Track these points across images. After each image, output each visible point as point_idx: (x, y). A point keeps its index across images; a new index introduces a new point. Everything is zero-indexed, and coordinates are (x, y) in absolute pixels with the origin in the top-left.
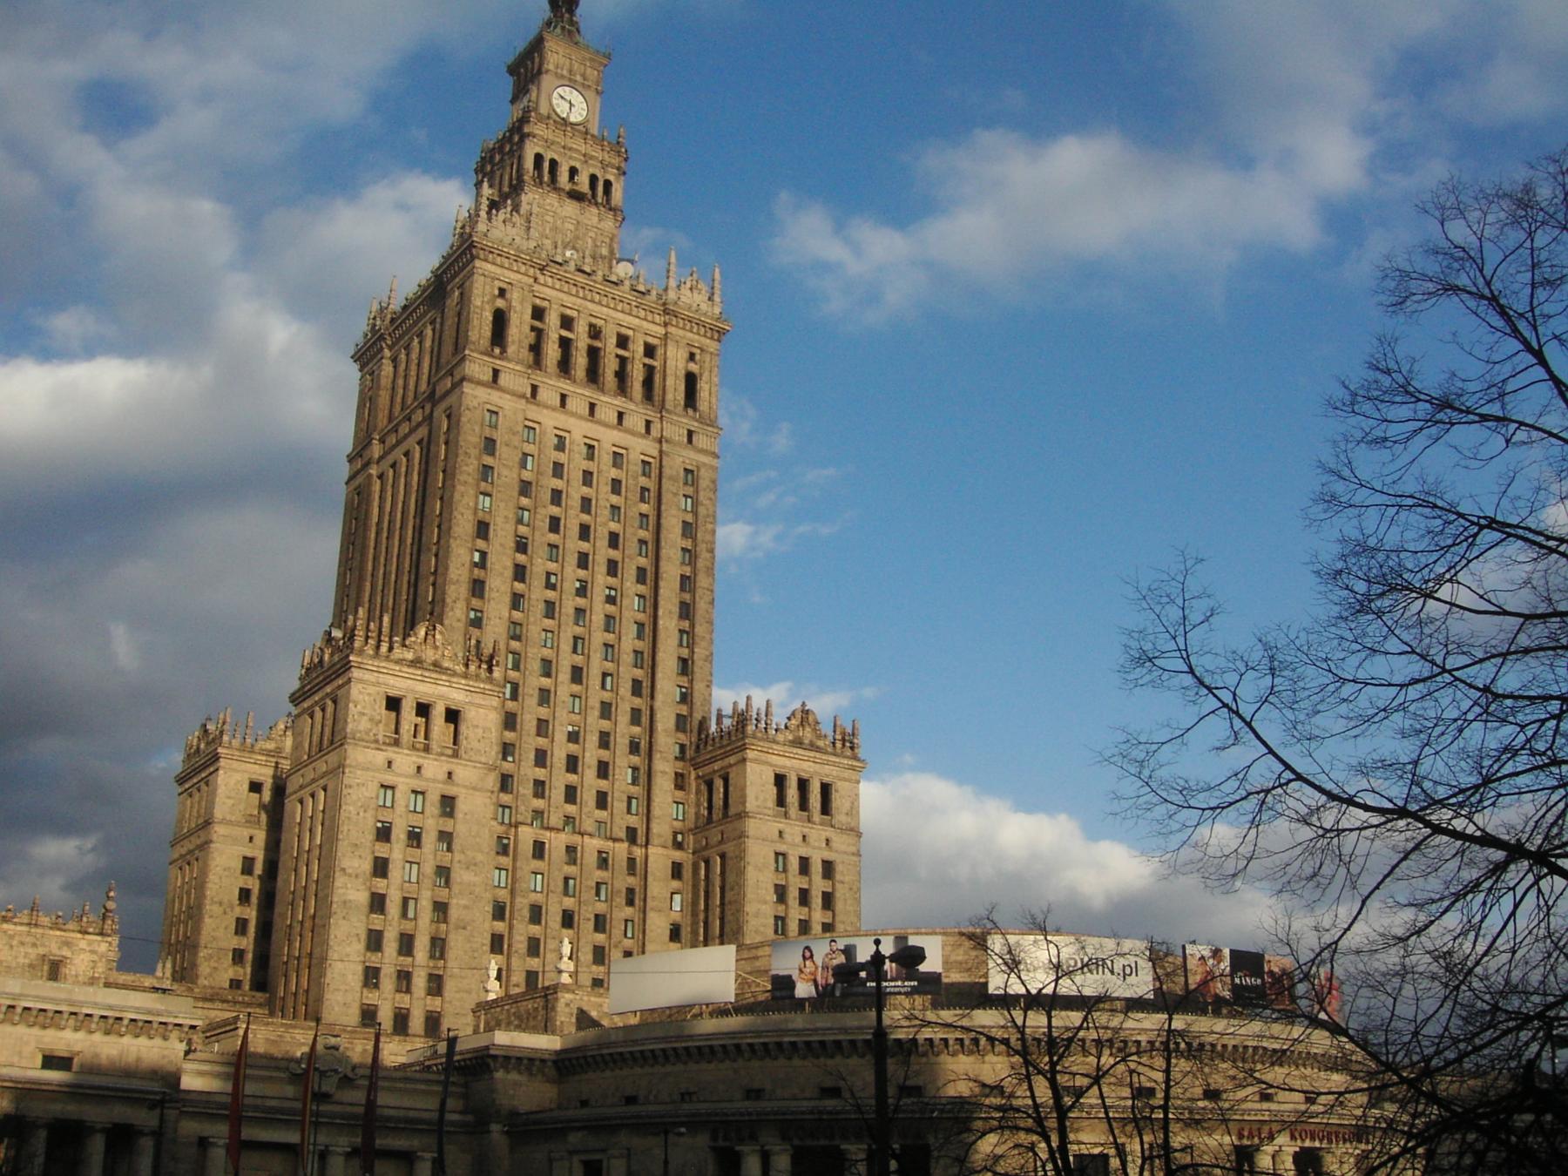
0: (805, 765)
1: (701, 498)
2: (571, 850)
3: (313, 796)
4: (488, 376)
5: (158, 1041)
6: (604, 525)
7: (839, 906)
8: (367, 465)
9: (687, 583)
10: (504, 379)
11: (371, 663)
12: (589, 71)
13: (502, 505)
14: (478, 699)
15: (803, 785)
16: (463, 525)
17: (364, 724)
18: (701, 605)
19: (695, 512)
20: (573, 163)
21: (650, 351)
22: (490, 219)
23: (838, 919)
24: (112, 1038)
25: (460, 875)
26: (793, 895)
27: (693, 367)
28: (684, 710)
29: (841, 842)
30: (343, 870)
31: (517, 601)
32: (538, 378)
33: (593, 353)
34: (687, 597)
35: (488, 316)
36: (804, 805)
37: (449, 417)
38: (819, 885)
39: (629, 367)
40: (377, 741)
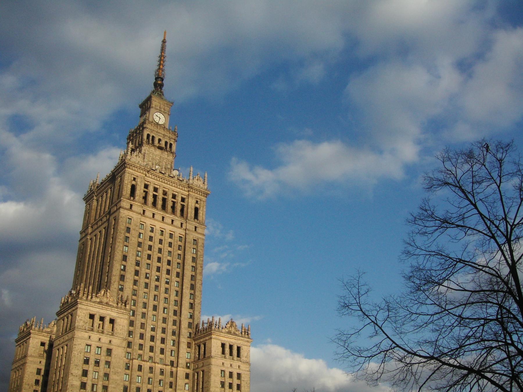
2: (151, 368)
3: (62, 348)
4: (129, 207)
6: (166, 257)
8: (86, 235)
9: (193, 277)
10: (134, 208)
11: (85, 303)
13: (132, 250)
15: (231, 347)
16: (118, 256)
17: (81, 323)
18: (198, 285)
19: (196, 254)
20: (160, 137)
21: (183, 200)
22: (131, 155)
25: (112, 376)
27: (197, 206)
28: (191, 321)
29: (244, 367)
30: (72, 374)
31: (135, 282)
32: (145, 208)
33: (164, 200)
34: (193, 282)
36: (231, 354)
37: (115, 220)
38: (236, 382)
39: (176, 205)
40: (85, 329)
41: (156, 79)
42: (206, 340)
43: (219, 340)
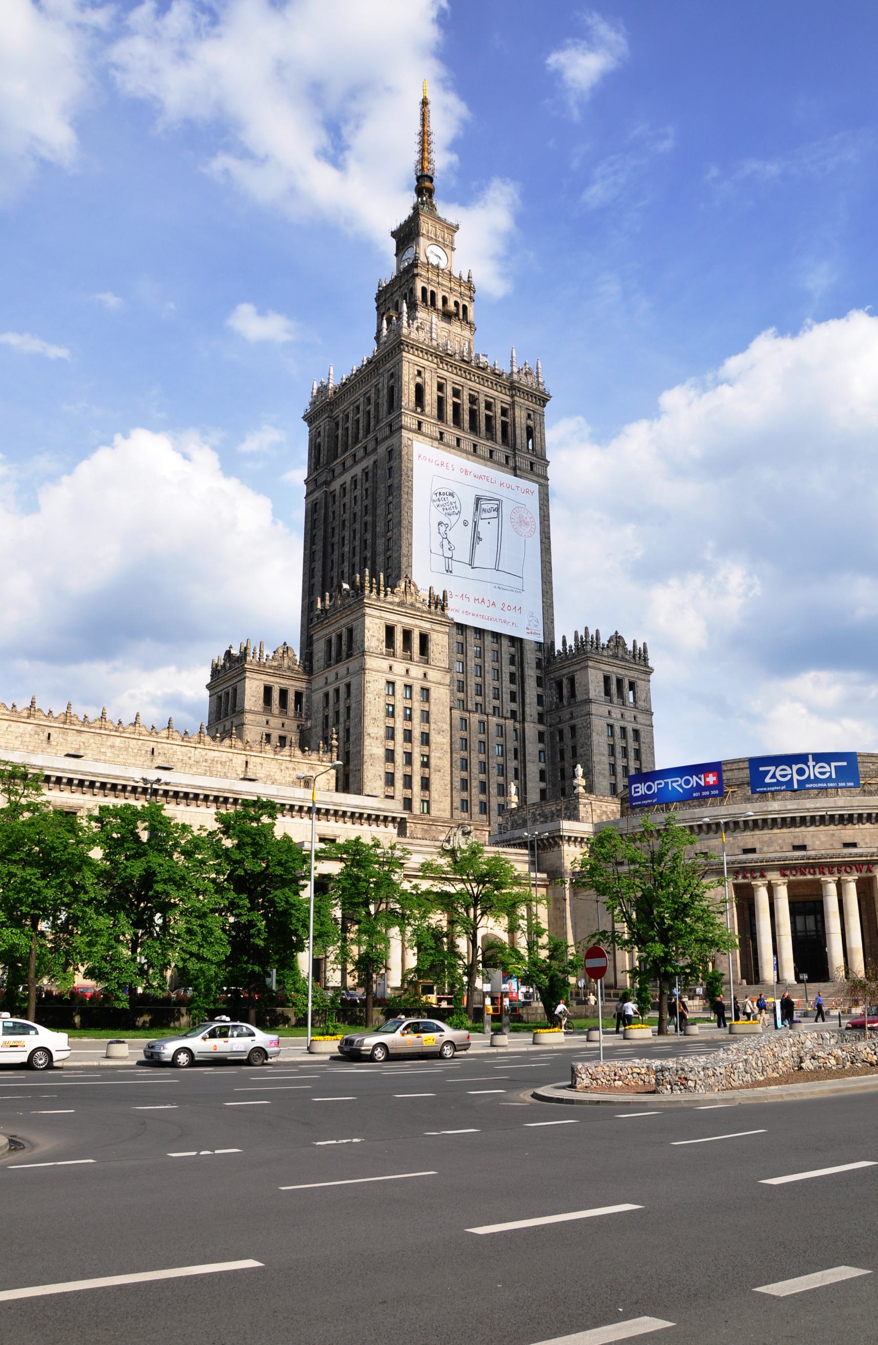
0: (620, 671)
2: (481, 722)
4: (415, 427)
10: (425, 428)
12: (446, 235)
14: (437, 627)
15: (619, 682)
20: (444, 294)
21: (504, 412)
22: (409, 326)
23: (643, 765)
25: (434, 738)
27: (531, 423)
29: (641, 718)
30: (369, 734)
33: (473, 414)
35: (413, 388)
41: (418, 179)
42: (576, 671)
43: (600, 669)
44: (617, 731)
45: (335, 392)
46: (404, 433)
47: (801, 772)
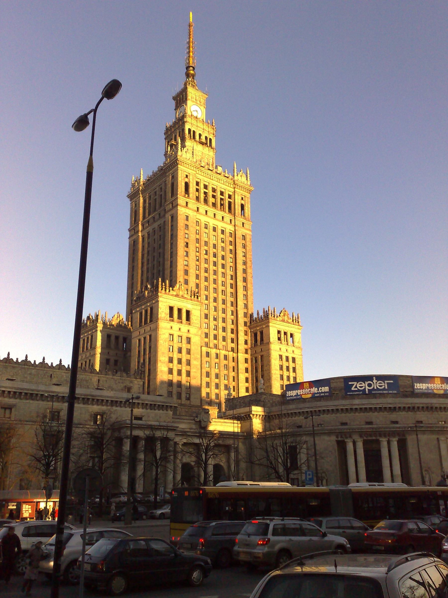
1: (247, 244)
2: (217, 354)
4: (185, 204)
5: (165, 411)
6: (220, 253)
7: (297, 371)
9: (245, 271)
10: (189, 205)
11: (165, 296)
18: (249, 278)
21: (230, 197)
22: (181, 151)
23: (297, 375)
24: (153, 411)
26: (285, 368)
27: (243, 202)
29: (297, 352)
30: (160, 361)
31: (197, 277)
32: (199, 205)
35: (183, 184)
37: (172, 217)
38: (292, 365)
44: (284, 358)
45: (144, 184)
46: (179, 208)
47: (370, 385)
